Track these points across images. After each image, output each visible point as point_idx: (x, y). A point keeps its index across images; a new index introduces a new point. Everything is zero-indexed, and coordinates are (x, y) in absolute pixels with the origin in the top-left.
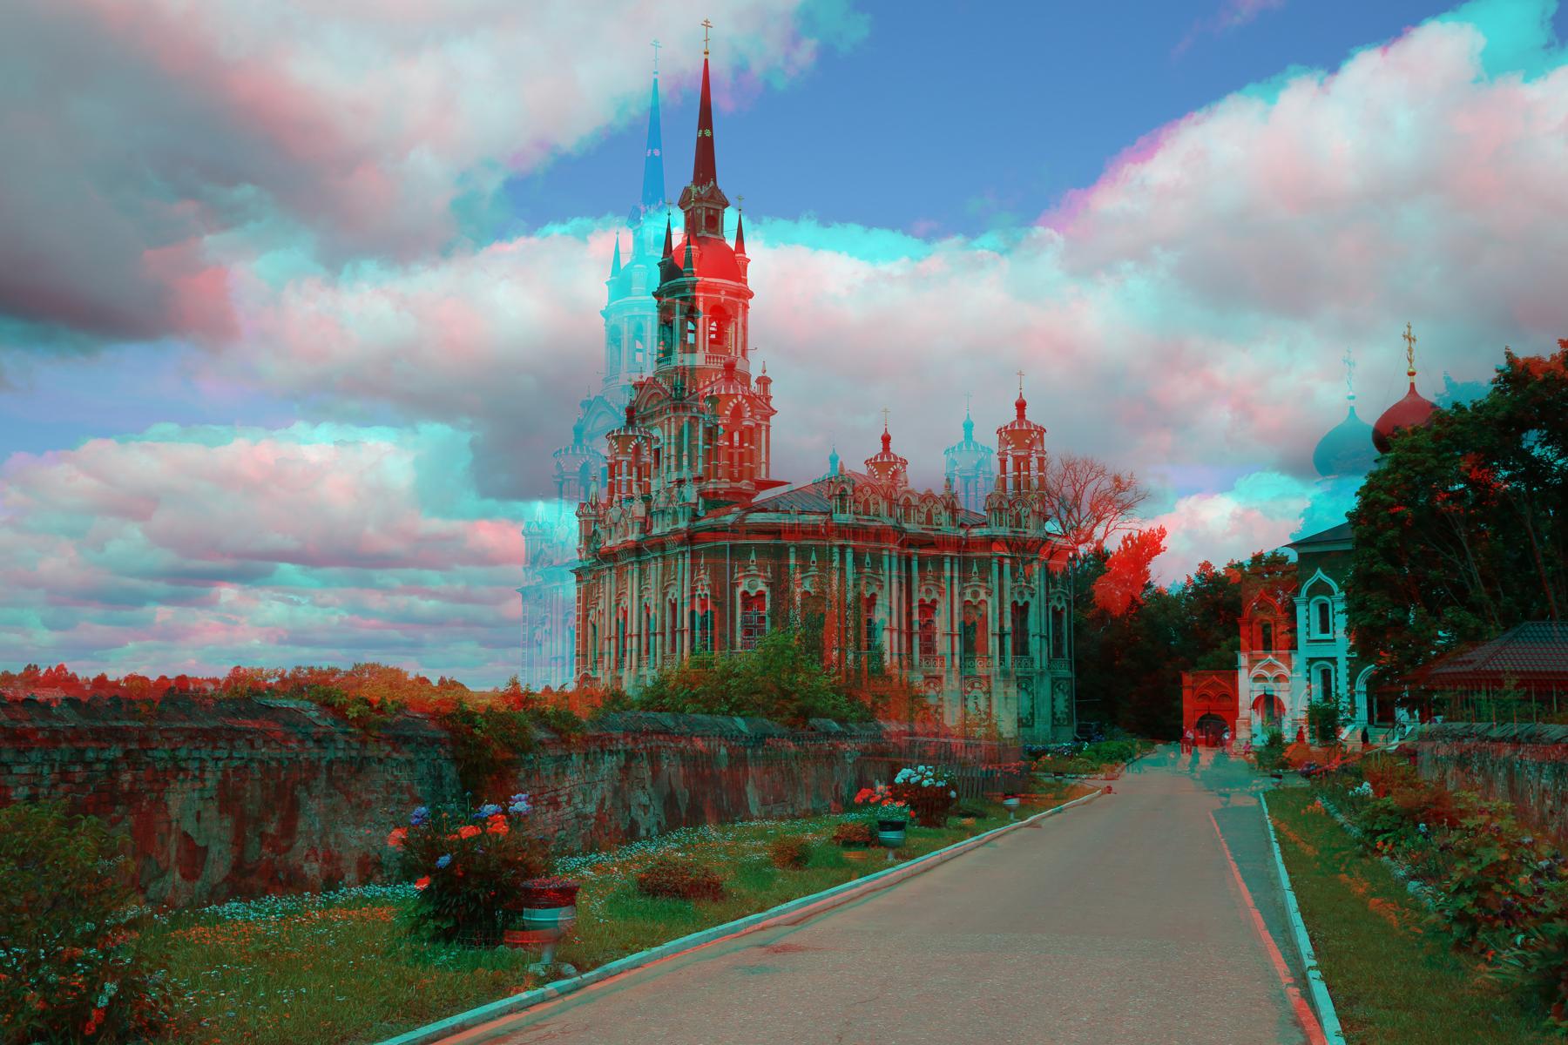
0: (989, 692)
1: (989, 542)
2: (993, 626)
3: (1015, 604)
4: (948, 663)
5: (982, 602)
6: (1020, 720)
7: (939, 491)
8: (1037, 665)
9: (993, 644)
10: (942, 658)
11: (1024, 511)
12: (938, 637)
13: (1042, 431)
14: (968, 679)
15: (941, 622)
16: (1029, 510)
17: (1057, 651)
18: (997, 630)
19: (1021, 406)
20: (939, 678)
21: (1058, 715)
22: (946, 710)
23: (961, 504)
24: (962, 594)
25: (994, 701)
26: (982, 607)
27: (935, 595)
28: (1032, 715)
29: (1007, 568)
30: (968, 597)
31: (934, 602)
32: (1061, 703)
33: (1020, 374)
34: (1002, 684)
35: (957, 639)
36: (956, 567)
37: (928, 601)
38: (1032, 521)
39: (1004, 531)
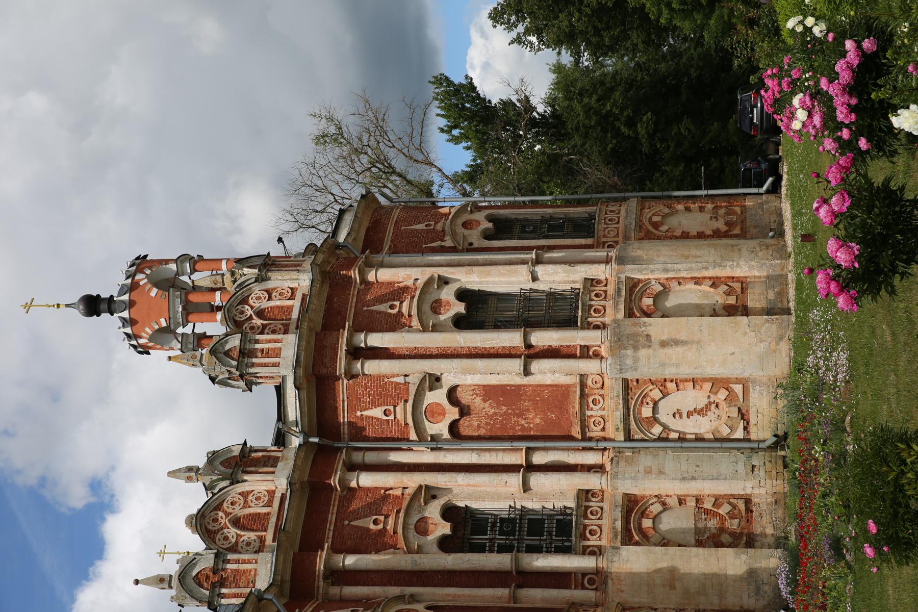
0: (662, 384)
1: (317, 380)
2: (508, 373)
3: (460, 323)
4: (592, 482)
5: (452, 395)
6: (730, 311)
7: (195, 497)
8: (599, 271)
9: (547, 373)
10: (585, 495)
11: (258, 300)
12: (533, 504)
13: (141, 263)
14: (639, 434)
15: (492, 495)
16: (257, 290)
17: (583, 228)
18: (516, 365)
19: (93, 305)
20: (632, 506)
21: (720, 225)
22: (708, 488)
23: (229, 439)
24: (435, 442)
25: (685, 371)
26: (464, 397)
27: (433, 511)
28: (715, 283)
29: (376, 340)
30: (441, 428)
31: (449, 512)
32: (692, 220)
33: (28, 307)
34: (643, 353)
35: (539, 459)
36: (371, 457)
37: (445, 528)
38: (280, 280)
39: (289, 345)
